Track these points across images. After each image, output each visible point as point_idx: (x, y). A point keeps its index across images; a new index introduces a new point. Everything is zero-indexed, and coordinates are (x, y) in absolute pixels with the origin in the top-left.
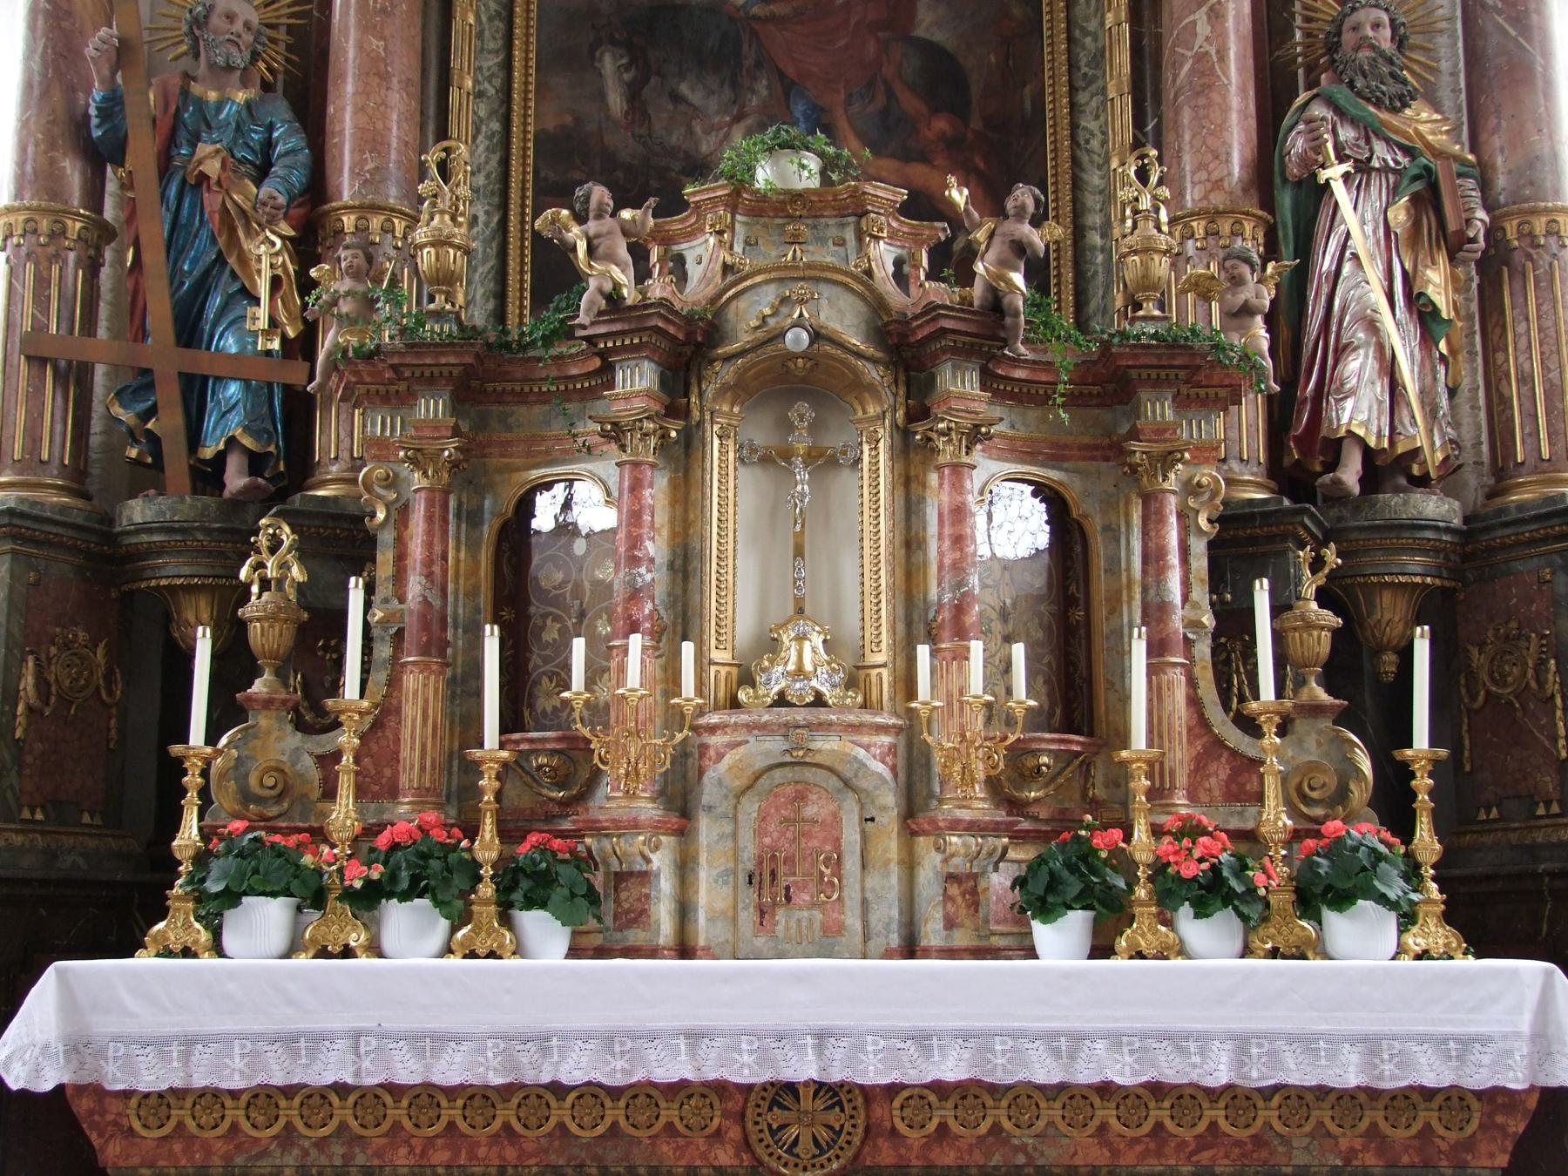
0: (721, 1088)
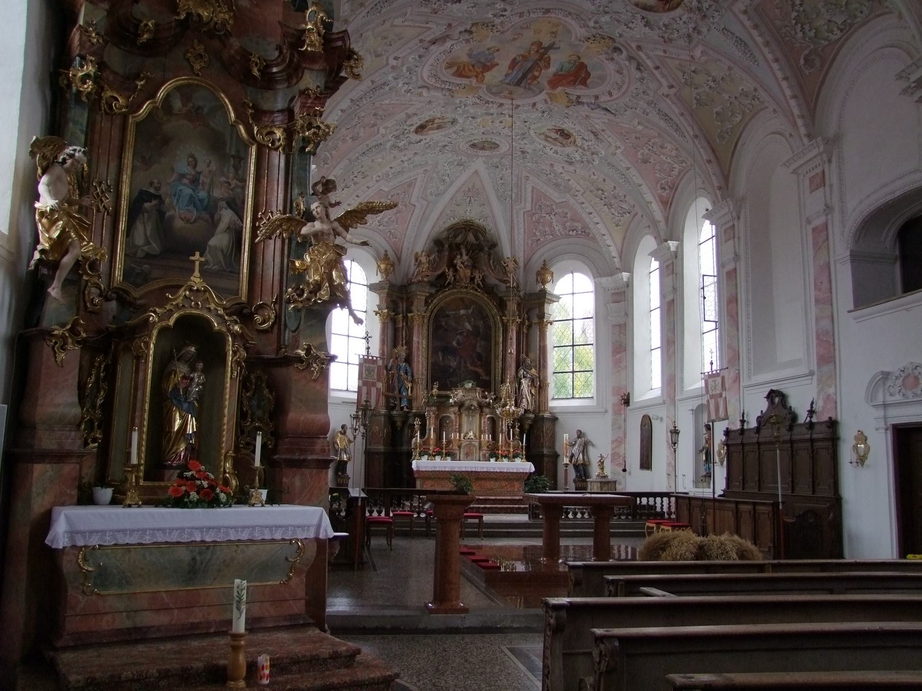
0: (467, 471)
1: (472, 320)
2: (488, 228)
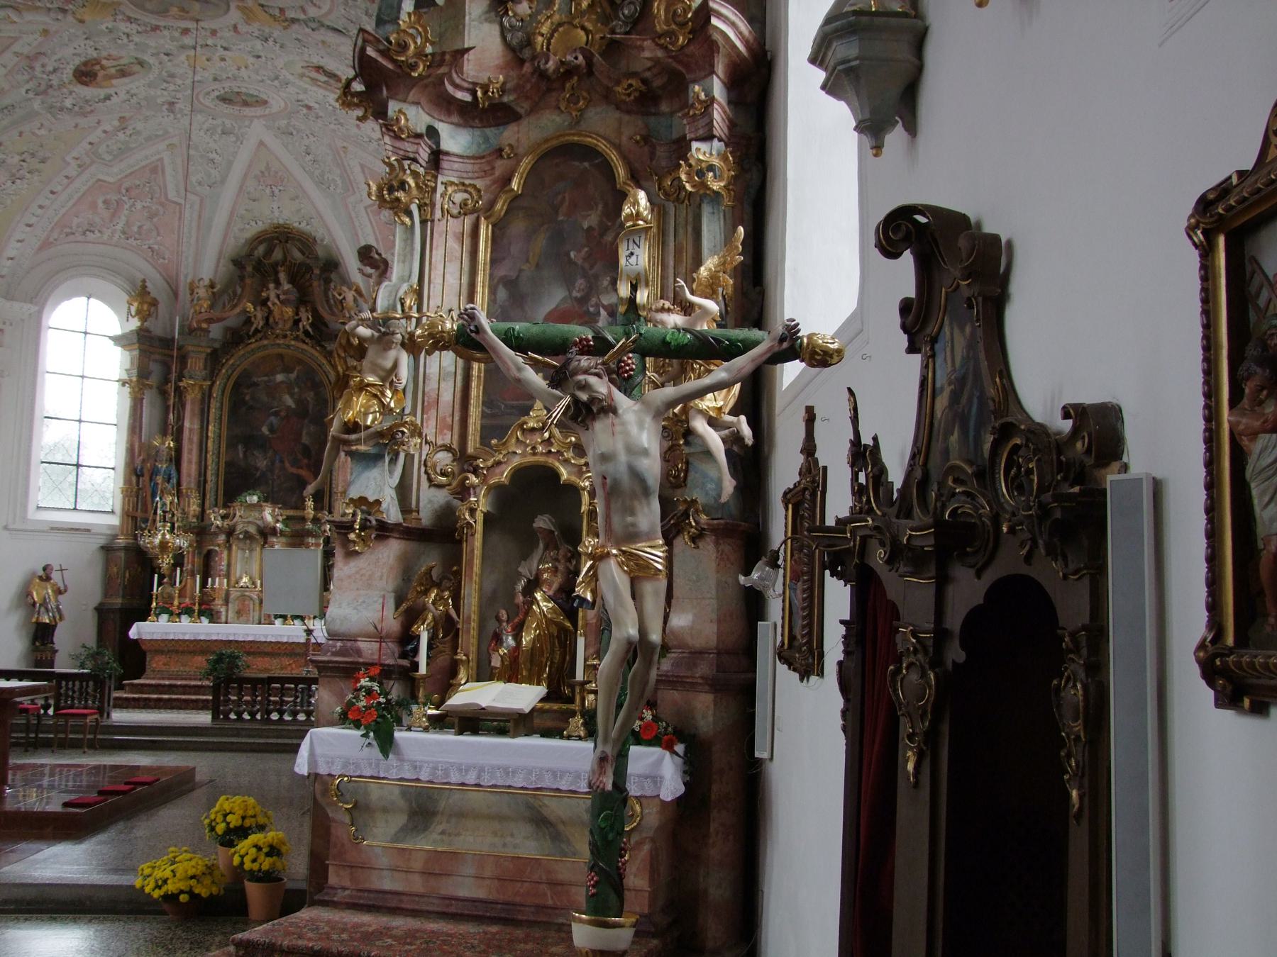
1: (296, 390)
2: (318, 236)
